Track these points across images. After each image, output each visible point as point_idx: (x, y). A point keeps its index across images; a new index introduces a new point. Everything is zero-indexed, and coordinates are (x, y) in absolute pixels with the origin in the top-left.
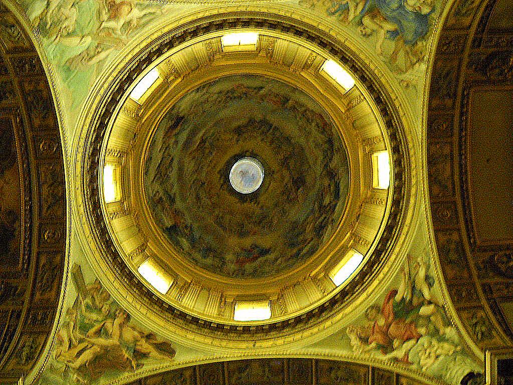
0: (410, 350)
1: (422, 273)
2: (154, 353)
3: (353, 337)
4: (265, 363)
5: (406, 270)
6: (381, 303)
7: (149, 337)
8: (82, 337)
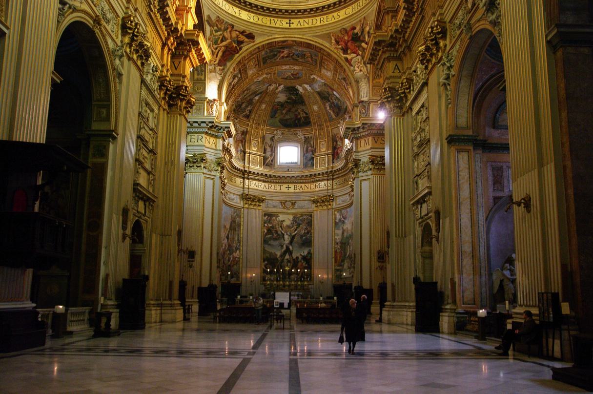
0: (353, 58)
1: (367, 29)
2: (246, 40)
3: (333, 38)
4: (293, 41)
5: (362, 22)
6: (348, 29)
7: (243, 33)
8: (216, 46)
